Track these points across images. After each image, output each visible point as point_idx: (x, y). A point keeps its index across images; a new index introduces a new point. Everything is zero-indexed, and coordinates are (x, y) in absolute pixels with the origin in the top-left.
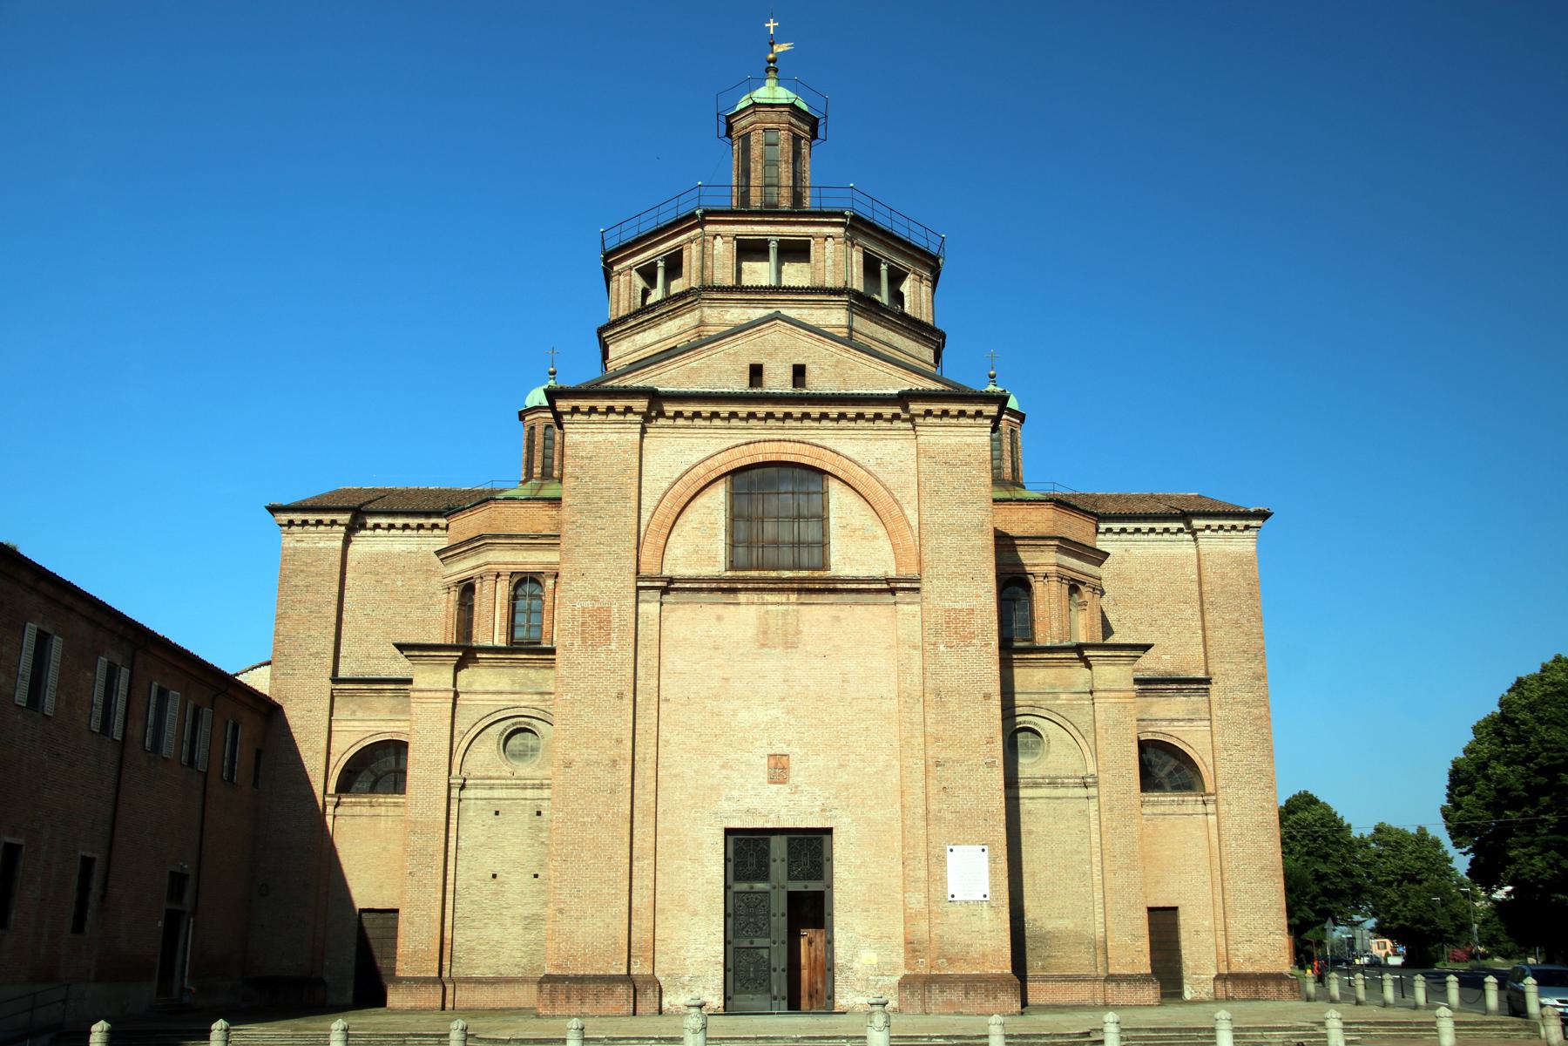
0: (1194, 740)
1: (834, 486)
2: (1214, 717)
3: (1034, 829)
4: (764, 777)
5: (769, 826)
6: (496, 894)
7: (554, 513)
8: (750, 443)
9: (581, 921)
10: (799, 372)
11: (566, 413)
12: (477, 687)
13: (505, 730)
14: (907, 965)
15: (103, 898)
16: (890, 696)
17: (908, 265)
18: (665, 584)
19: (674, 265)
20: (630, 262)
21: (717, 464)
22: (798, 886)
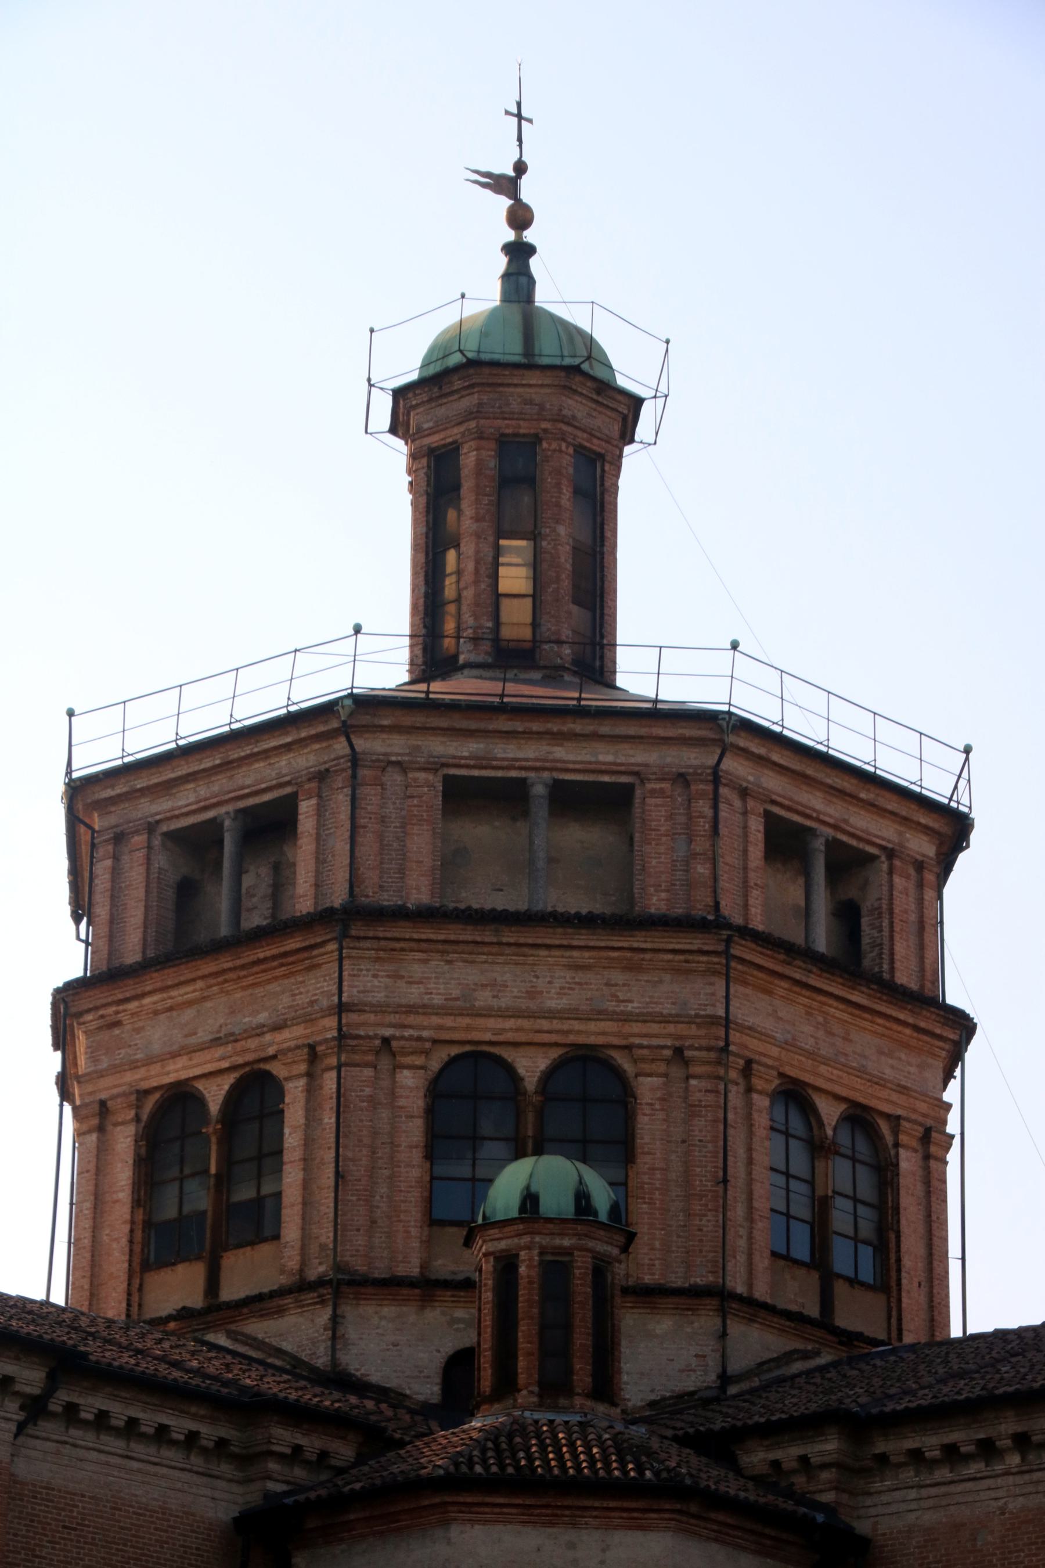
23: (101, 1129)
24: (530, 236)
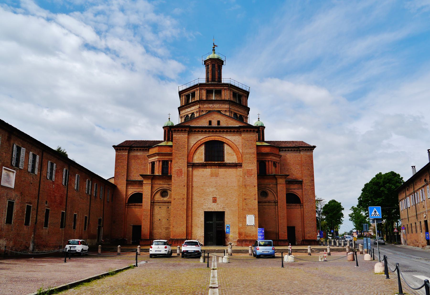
0: (298, 192)
1: (225, 145)
2: (303, 189)
3: (265, 211)
4: (212, 201)
5: (213, 211)
6: (160, 223)
7: (170, 148)
8: (209, 136)
9: (177, 229)
10: (219, 122)
11: (173, 131)
12: (156, 183)
13: (161, 191)
14: (239, 238)
15: (89, 224)
16: (236, 186)
17: (242, 93)
18: (192, 164)
19: (193, 95)
20: (184, 94)
21: (203, 141)
22: (218, 222)
23: (182, 118)
24: (214, 49)
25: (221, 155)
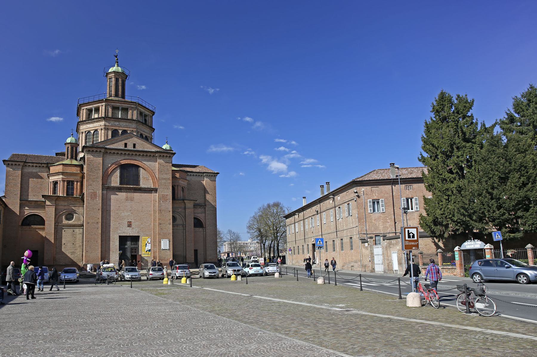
10: (134, 146)
19: (97, 110)
20: (86, 107)
25: (136, 180)
